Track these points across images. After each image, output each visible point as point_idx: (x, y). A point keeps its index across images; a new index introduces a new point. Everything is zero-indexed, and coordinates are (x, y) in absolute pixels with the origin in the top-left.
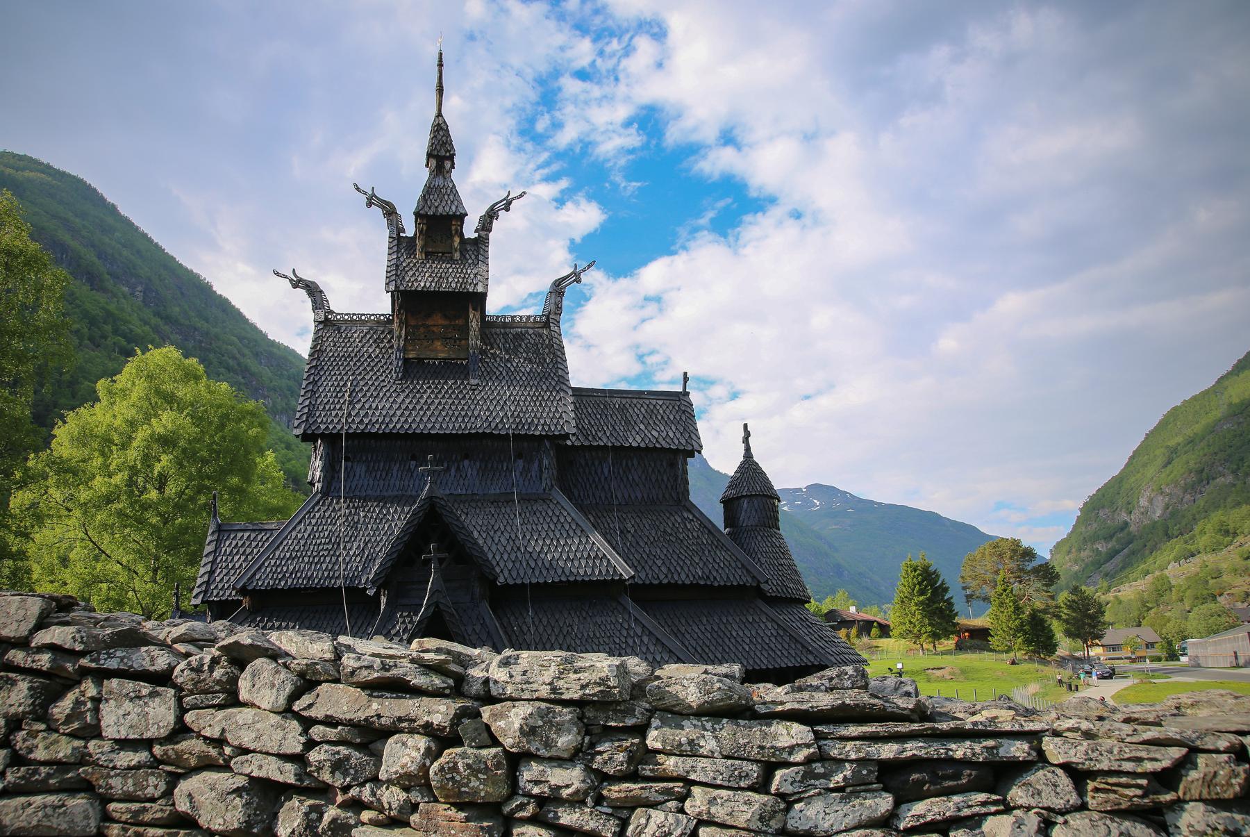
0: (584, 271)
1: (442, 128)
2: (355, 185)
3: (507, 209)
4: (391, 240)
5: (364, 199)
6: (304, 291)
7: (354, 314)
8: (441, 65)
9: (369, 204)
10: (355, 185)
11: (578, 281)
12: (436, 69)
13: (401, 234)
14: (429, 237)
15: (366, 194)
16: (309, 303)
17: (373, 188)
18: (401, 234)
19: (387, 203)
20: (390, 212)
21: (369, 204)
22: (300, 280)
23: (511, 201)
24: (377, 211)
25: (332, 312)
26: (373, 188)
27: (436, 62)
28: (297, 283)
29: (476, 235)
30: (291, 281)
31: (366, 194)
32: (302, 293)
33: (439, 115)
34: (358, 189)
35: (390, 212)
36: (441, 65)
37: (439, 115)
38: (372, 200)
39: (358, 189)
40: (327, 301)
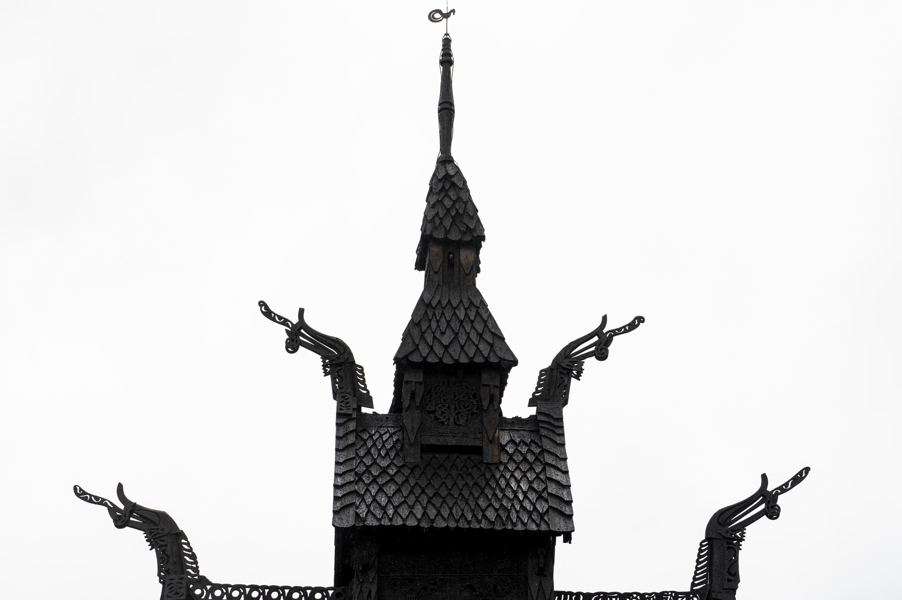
0: (783, 489)
1: (453, 185)
2: (262, 304)
3: (601, 353)
4: (342, 421)
5: (281, 334)
6: (140, 536)
7: (254, 588)
8: (447, 61)
9: (292, 345)
10: (262, 304)
11: (773, 512)
12: (438, 71)
13: (364, 410)
14: (429, 412)
15: (284, 322)
16: (150, 558)
17: (301, 311)
18: (364, 410)
19: (337, 344)
21: (292, 345)
23: (608, 341)
26: (301, 311)
29: (533, 411)
30: (113, 510)
32: (136, 538)
33: (445, 159)
34: (268, 313)
36: (447, 61)
37: (445, 159)
39: (268, 313)
40: (193, 557)
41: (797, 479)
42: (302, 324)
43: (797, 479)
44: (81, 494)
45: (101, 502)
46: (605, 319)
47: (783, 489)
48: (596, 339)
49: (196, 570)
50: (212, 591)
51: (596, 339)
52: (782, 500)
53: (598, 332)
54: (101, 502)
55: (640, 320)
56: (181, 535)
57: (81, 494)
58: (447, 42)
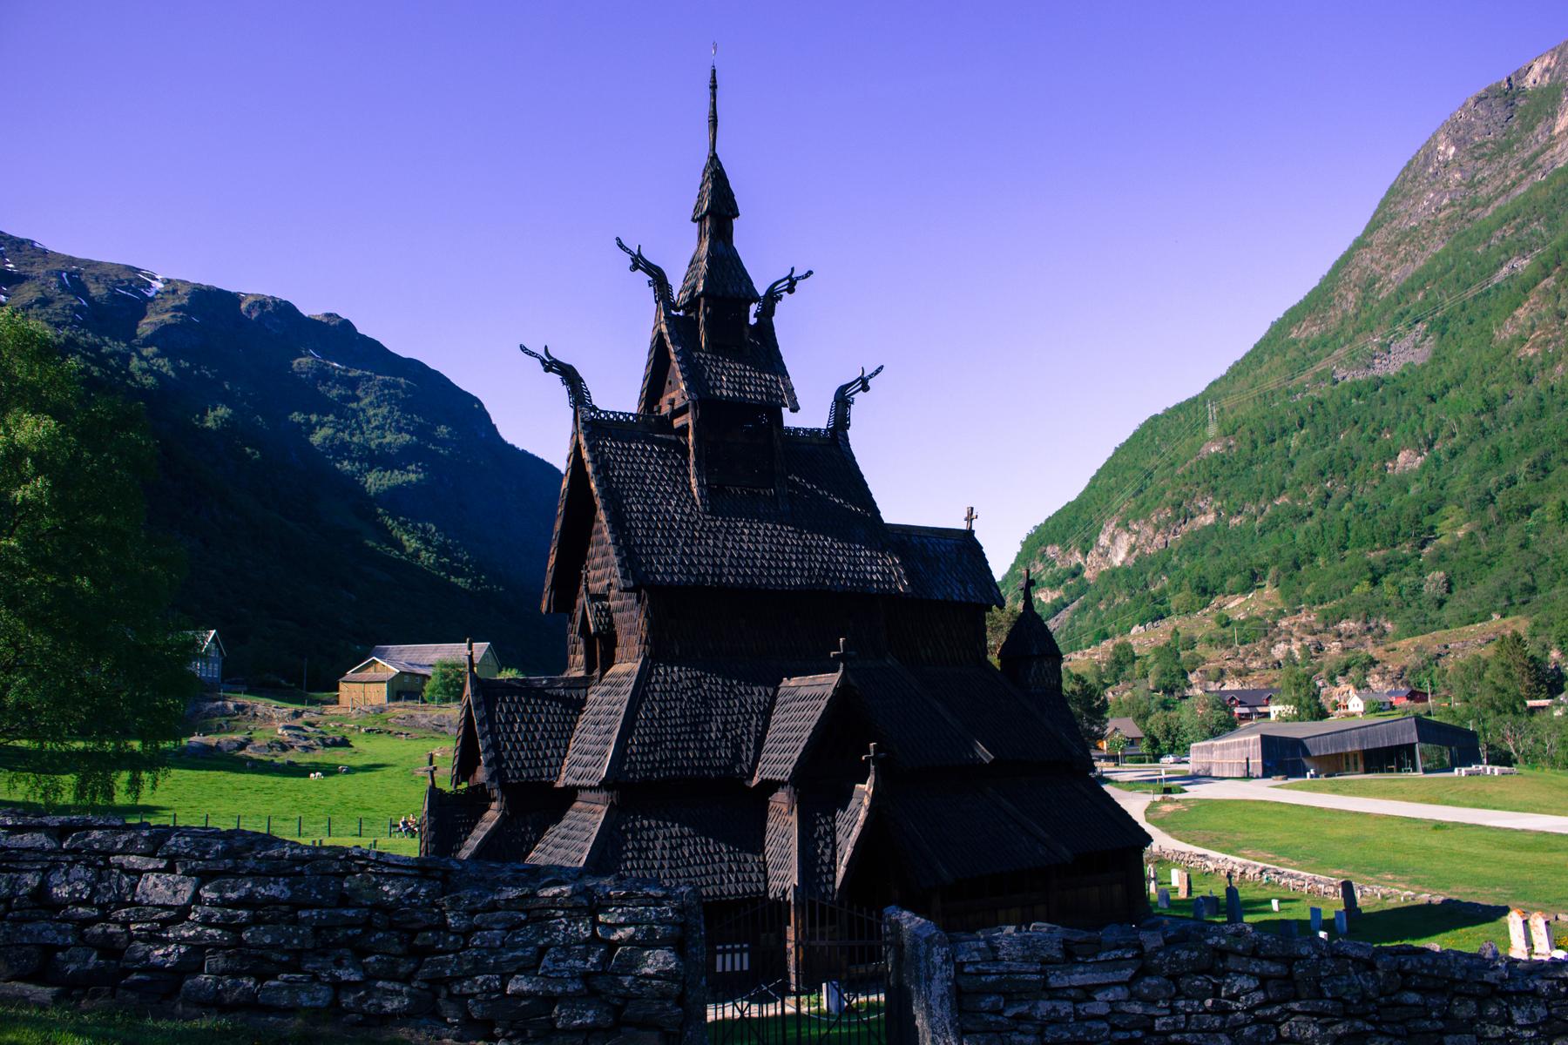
0: (870, 377)
2: (618, 239)
3: (791, 290)
5: (627, 260)
7: (620, 413)
8: (714, 87)
9: (635, 267)
10: (618, 239)
11: (865, 388)
12: (709, 91)
15: (630, 252)
16: (563, 391)
20: (659, 280)
21: (635, 267)
22: (556, 362)
23: (795, 283)
24: (643, 277)
25: (594, 408)
27: (708, 83)
28: (551, 365)
30: (543, 362)
31: (630, 252)
32: (555, 379)
34: (621, 245)
35: (659, 280)
36: (714, 87)
38: (639, 262)
39: (621, 245)
40: (588, 393)
41: (877, 372)
42: (640, 255)
43: (877, 372)
44: (523, 348)
45: (536, 356)
46: (793, 269)
47: (870, 377)
48: (788, 281)
49: (590, 401)
50: (599, 415)
51: (788, 281)
52: (871, 383)
53: (789, 277)
54: (536, 356)
55: (810, 273)
56: (581, 380)
57: (523, 348)
58: (714, 71)
